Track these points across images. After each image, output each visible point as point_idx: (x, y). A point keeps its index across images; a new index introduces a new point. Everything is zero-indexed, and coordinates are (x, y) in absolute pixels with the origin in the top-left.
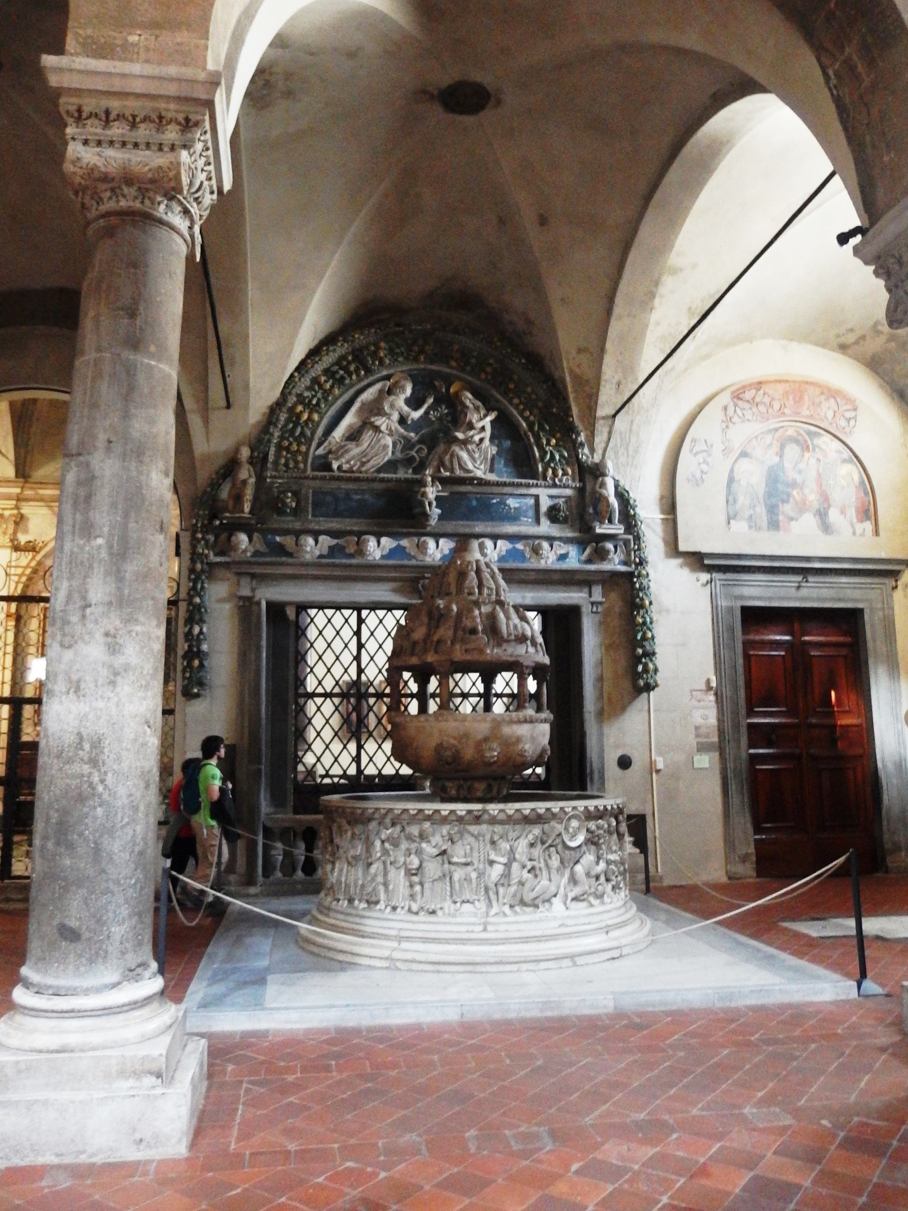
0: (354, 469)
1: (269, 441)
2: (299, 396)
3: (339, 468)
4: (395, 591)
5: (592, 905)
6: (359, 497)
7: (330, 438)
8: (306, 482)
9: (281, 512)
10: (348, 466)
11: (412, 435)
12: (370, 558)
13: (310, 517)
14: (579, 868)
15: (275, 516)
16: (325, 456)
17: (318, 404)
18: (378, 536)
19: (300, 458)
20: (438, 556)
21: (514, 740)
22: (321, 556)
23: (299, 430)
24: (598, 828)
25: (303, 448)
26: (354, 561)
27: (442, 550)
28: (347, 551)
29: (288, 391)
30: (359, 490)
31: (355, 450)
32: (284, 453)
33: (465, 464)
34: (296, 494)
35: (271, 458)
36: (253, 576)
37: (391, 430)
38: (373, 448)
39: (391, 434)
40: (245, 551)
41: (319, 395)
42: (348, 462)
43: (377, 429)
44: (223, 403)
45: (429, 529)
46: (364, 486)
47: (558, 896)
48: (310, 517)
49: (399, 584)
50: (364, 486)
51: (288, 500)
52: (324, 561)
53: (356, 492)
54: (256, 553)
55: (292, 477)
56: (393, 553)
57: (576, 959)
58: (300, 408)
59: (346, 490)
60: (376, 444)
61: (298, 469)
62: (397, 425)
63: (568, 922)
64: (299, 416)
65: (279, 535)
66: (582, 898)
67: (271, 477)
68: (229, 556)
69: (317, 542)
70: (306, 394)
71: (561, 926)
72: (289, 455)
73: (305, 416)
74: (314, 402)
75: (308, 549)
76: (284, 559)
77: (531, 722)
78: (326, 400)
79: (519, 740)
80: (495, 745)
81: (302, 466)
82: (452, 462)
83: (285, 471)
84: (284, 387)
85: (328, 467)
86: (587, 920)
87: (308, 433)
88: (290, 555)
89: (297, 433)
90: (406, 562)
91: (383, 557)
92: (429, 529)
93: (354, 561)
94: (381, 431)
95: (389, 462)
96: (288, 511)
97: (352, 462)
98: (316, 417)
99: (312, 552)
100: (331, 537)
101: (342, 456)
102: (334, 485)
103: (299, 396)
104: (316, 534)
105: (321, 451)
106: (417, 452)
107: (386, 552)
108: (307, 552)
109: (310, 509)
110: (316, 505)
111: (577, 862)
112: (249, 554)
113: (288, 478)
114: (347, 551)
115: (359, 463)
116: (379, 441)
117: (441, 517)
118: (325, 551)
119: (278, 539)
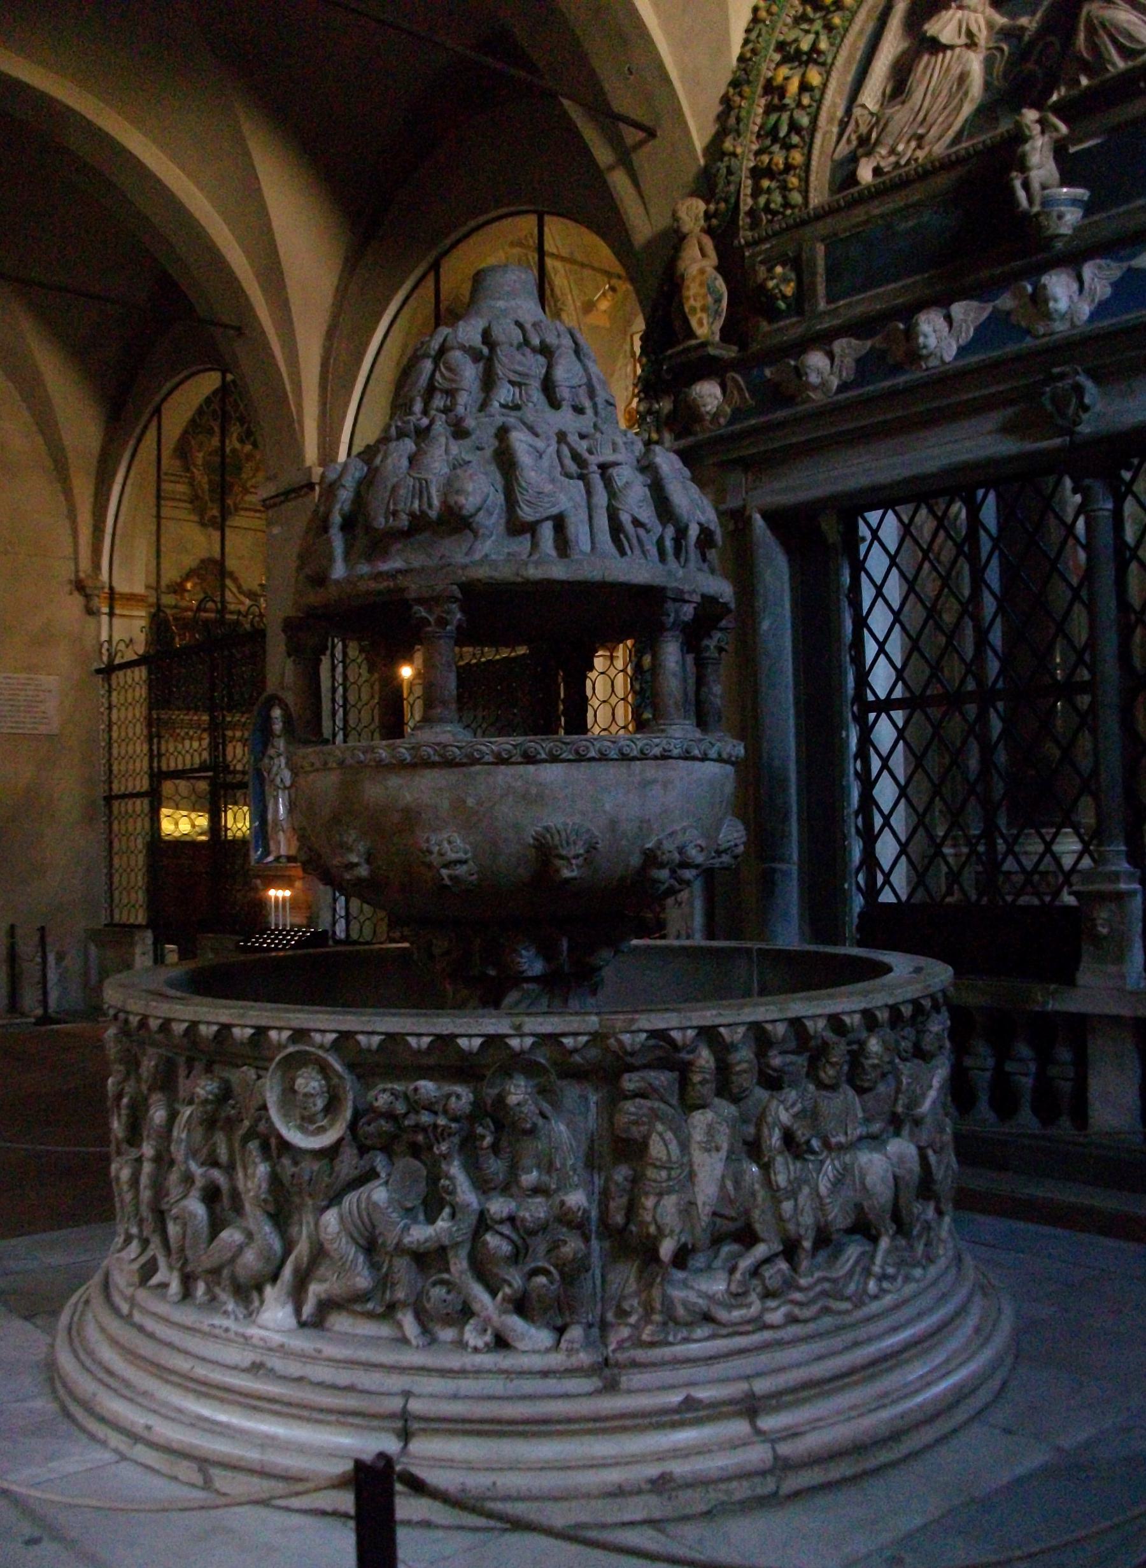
0: (903, 162)
1: (730, 172)
2: (781, 46)
3: (877, 171)
4: (1007, 429)
5: (404, 1341)
6: (910, 224)
7: (857, 112)
8: (808, 231)
9: (773, 315)
10: (893, 159)
11: (1024, 21)
12: (933, 362)
13: (822, 305)
14: (331, 1218)
15: (765, 326)
16: (853, 159)
17: (814, 48)
18: (943, 301)
19: (793, 181)
20: (1085, 309)
21: (396, 817)
22: (843, 387)
23: (785, 116)
24: (415, 1105)
25: (797, 157)
26: (901, 380)
27: (1093, 292)
28: (890, 361)
29: (750, 46)
30: (907, 207)
31: (901, 116)
32: (766, 183)
33: (1130, 37)
34: (798, 265)
35: (746, 203)
36: (747, 464)
37: (970, 34)
38: (935, 97)
39: (972, 44)
40: (716, 416)
41: (818, 25)
42: (892, 151)
43: (935, 46)
44: (641, 135)
45: (1059, 245)
46: (916, 194)
47: (279, 1282)
48: (822, 305)
49: (1010, 411)
50: (916, 194)
51: (771, 284)
52: (841, 397)
53: (906, 211)
54: (738, 414)
55: (782, 231)
56: (984, 334)
57: (214, 1472)
58: (784, 71)
59: (882, 216)
60: (939, 83)
61: (793, 207)
62: (990, 11)
63: (276, 1363)
64: (782, 91)
65: (771, 364)
66: (358, 1308)
67: (748, 244)
68: (695, 434)
69: (831, 356)
70: (791, 36)
71: (256, 1368)
72: (774, 185)
73: (793, 87)
74: (805, 46)
75: (814, 379)
76: (780, 415)
77: (450, 763)
78: (829, 27)
79: (411, 818)
80: (351, 837)
81: (796, 198)
82: (1095, 49)
83: (770, 222)
84: (746, 42)
85: (851, 179)
86: (344, 1377)
87: (805, 121)
88: (789, 400)
89: (783, 131)
90: (1011, 348)
91: (962, 351)
92: (1059, 245)
93: (901, 380)
94: (945, 48)
95: (979, 111)
96: (782, 305)
97: (900, 148)
98: (815, 77)
99: (824, 384)
100: (858, 338)
101: (878, 142)
102: (859, 214)
103: (781, 46)
104: (823, 340)
105: (843, 149)
106: (1038, 62)
107: (968, 333)
108: (815, 388)
109: (821, 289)
110: (833, 273)
111: (335, 1199)
112: (722, 421)
113: (775, 234)
114: (890, 361)
115: (913, 144)
116: (948, 69)
117: (1089, 208)
118: (848, 374)
119: (767, 373)
